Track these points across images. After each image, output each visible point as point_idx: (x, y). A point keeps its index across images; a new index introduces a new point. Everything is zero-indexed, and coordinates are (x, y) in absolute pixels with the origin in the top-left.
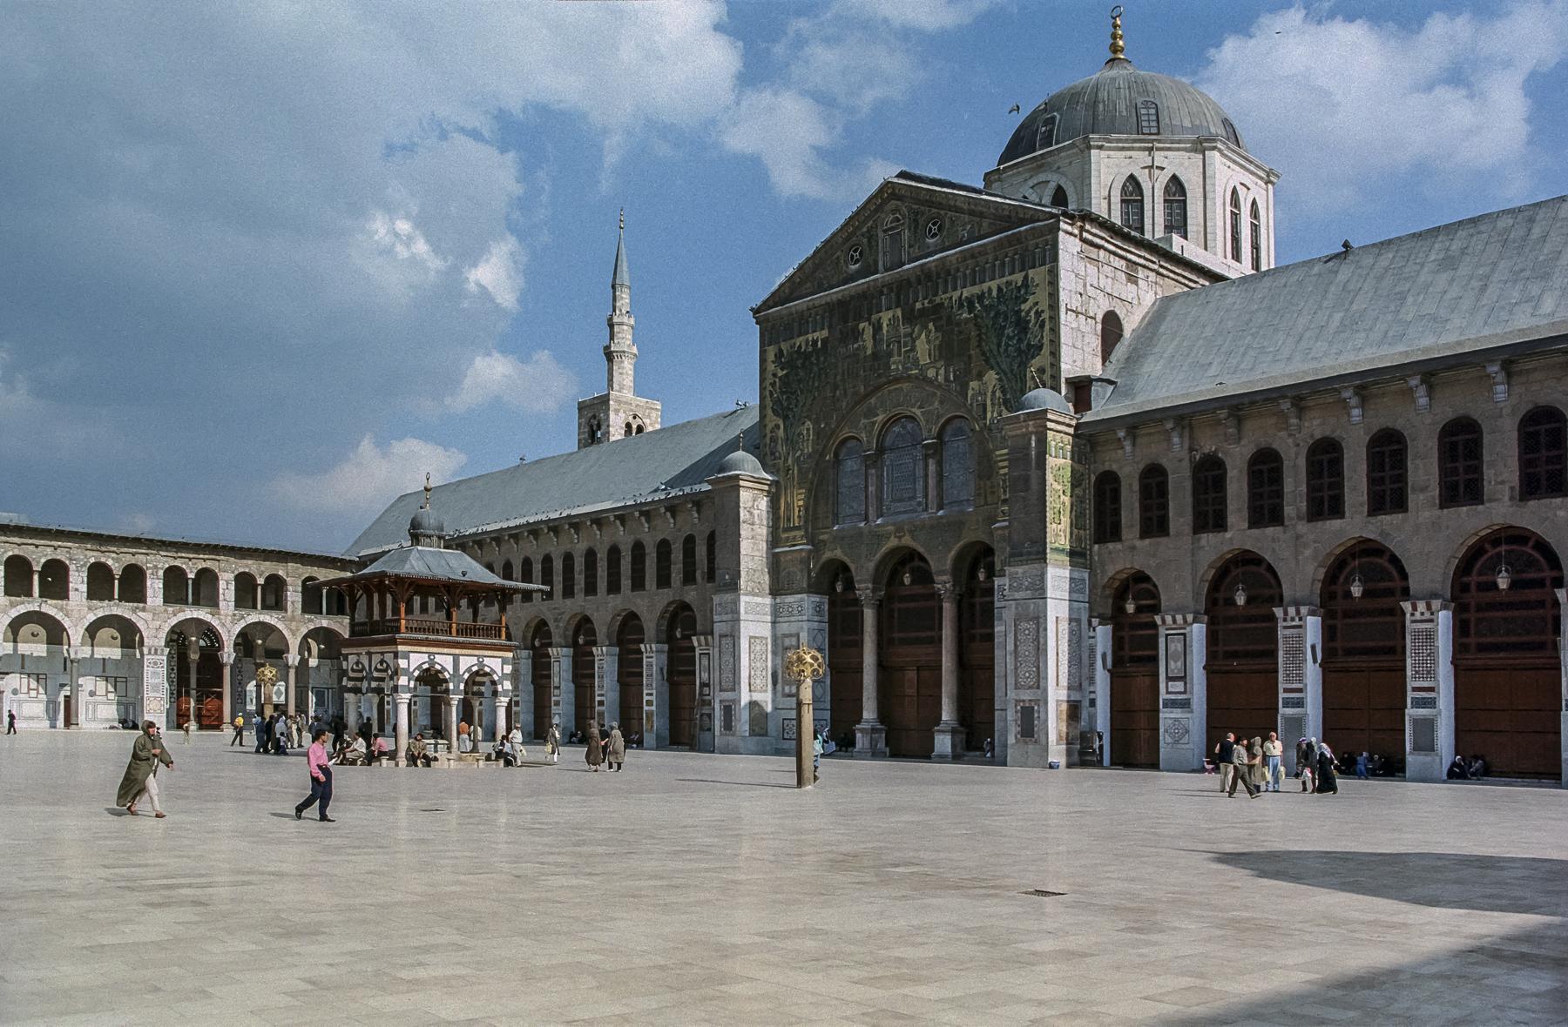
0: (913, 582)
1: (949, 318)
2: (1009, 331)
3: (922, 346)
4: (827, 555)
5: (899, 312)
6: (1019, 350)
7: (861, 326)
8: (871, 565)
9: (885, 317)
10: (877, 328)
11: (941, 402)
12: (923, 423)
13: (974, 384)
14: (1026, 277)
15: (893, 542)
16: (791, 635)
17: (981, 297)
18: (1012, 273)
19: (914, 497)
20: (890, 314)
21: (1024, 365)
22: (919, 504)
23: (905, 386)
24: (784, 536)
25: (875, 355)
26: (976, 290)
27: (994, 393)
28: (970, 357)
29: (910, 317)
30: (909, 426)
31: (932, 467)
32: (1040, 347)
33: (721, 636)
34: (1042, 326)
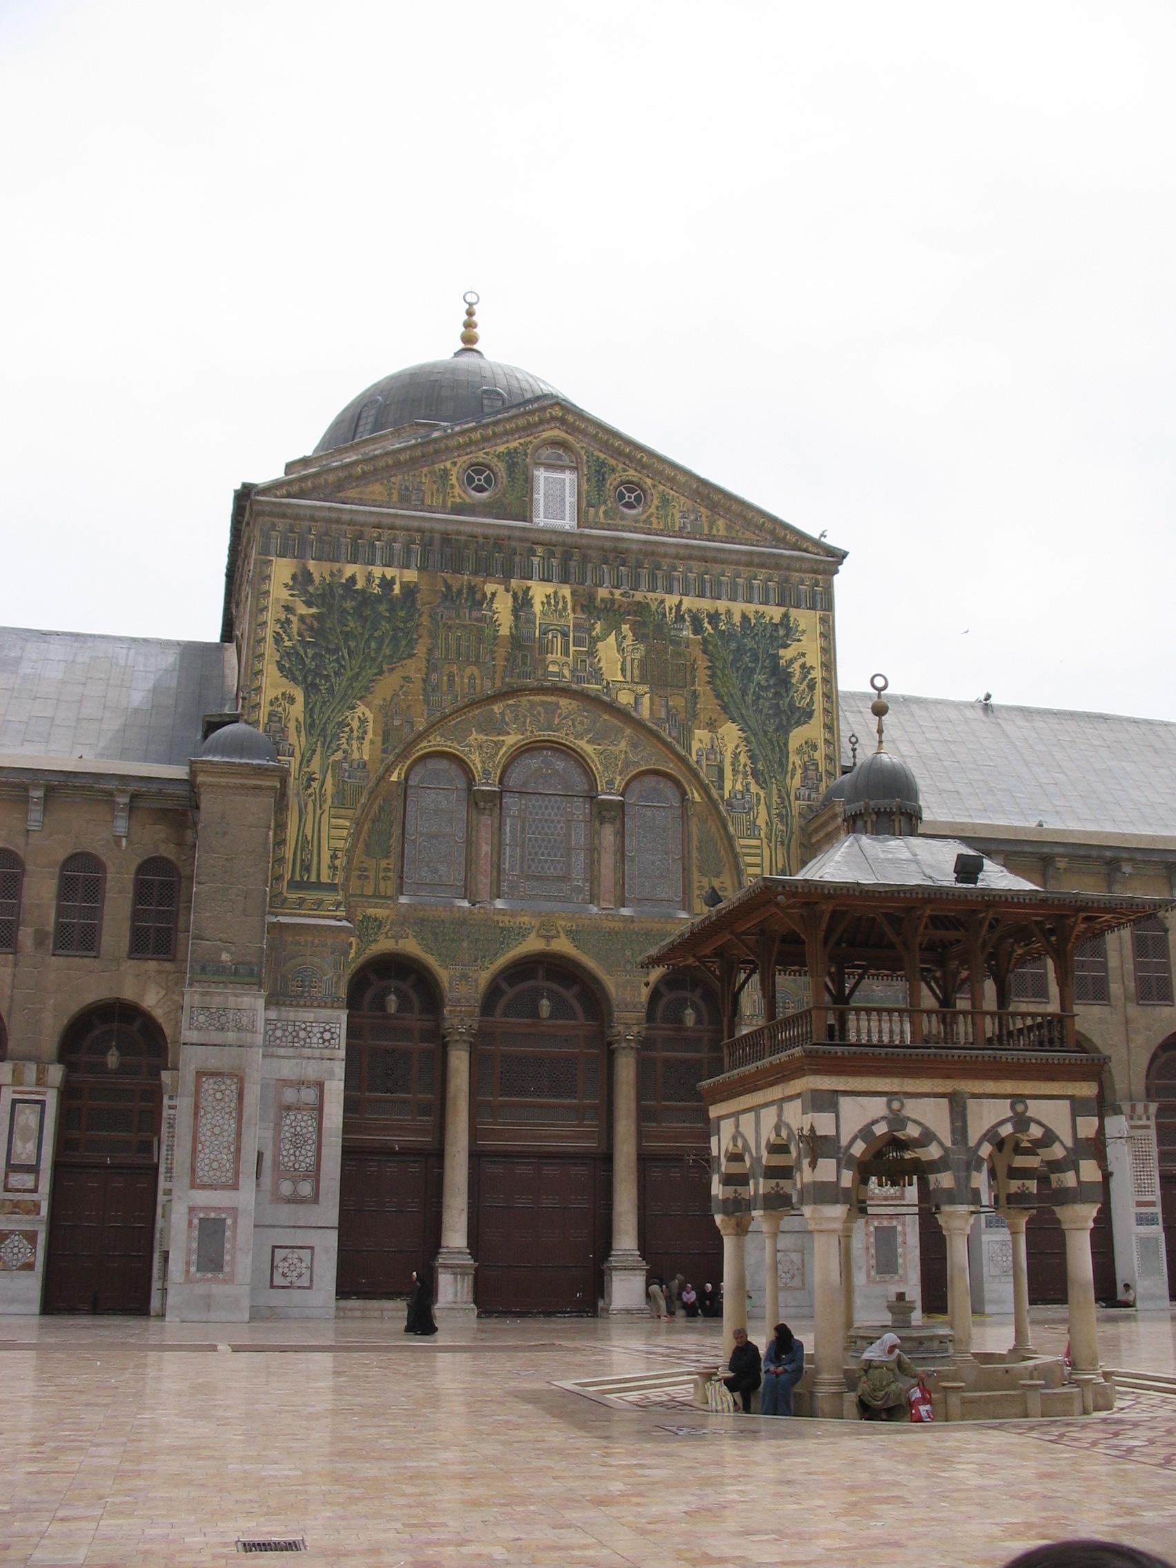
0: (550, 1017)
1: (660, 628)
2: (760, 677)
3: (613, 656)
4: (384, 945)
5: (566, 591)
6: (778, 712)
7: (489, 588)
8: (484, 977)
9: (539, 591)
10: (522, 603)
11: (634, 746)
12: (596, 766)
13: (701, 736)
14: (786, 616)
15: (532, 944)
16: (301, 1083)
17: (714, 618)
18: (766, 603)
19: (564, 878)
20: (549, 589)
21: (784, 730)
22: (579, 890)
23: (563, 702)
24: (293, 896)
25: (517, 641)
26: (705, 605)
27: (736, 755)
28: (695, 694)
29: (587, 604)
30: (560, 765)
31: (608, 835)
32: (810, 715)
33: (200, 1074)
34: (811, 687)
